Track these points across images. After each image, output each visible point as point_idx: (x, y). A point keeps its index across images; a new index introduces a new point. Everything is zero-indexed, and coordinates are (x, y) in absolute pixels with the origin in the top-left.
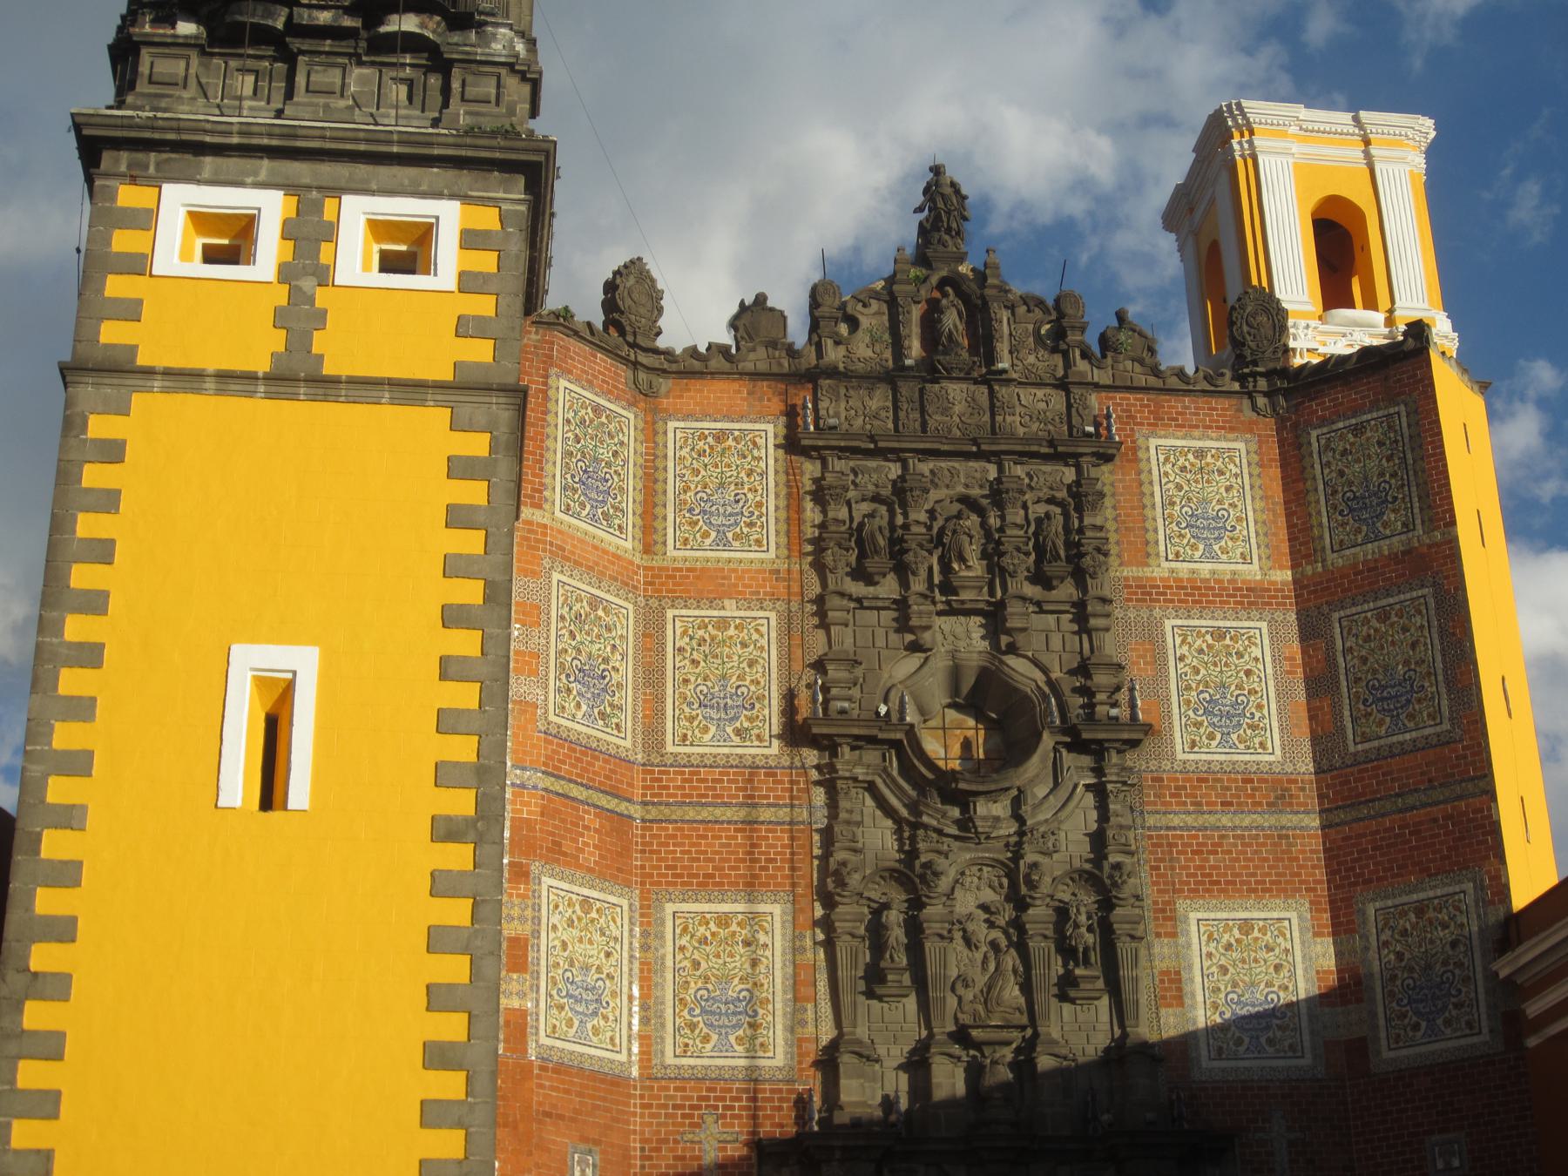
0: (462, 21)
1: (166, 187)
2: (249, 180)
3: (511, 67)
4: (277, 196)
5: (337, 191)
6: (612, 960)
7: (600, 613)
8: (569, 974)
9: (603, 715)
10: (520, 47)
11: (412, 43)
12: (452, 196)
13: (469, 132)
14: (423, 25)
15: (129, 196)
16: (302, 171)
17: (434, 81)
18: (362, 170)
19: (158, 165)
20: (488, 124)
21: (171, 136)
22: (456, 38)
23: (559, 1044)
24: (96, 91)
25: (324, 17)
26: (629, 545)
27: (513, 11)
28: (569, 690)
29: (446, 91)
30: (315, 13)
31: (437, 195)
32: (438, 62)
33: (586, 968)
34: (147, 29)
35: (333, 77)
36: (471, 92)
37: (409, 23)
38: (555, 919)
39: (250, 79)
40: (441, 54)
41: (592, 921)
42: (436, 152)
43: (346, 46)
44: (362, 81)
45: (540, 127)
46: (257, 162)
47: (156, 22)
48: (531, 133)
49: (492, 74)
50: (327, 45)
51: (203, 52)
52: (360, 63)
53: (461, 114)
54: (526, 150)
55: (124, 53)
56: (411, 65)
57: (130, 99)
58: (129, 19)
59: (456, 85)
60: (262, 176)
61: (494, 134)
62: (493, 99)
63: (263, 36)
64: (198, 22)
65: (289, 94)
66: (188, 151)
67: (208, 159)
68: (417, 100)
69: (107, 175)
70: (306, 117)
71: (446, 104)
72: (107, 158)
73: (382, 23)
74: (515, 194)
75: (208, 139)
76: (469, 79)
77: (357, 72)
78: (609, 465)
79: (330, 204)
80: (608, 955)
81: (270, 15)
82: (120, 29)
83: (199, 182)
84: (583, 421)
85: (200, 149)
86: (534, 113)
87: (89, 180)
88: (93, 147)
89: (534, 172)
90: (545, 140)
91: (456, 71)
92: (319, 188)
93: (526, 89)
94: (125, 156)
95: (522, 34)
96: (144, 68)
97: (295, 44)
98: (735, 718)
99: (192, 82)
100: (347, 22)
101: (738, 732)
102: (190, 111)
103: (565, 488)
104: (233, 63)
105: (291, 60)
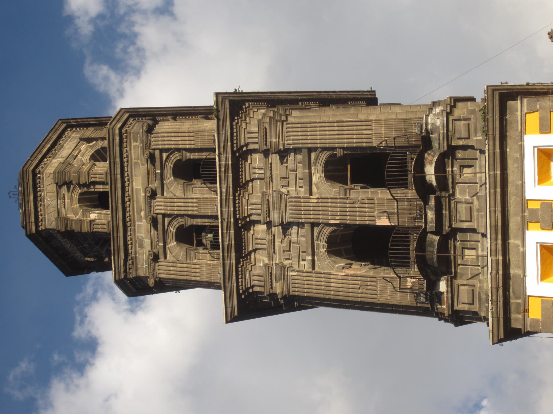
0: (426, 142)
1: (529, 293)
2: (521, 249)
3: (448, 114)
4: (528, 234)
5: (524, 202)
10: (437, 110)
11: (440, 168)
12: (522, 140)
13: (485, 133)
14: (431, 163)
15: (535, 312)
16: (514, 222)
17: (460, 154)
18: (511, 189)
19: (517, 298)
20: (481, 123)
21: (501, 292)
22: (435, 145)
24: (480, 332)
25: (431, 215)
27: (419, 115)
29: (465, 148)
30: (429, 220)
31: (522, 148)
32: (450, 153)
34: (445, 307)
35: (462, 208)
36: (464, 134)
37: (430, 170)
39: (467, 252)
40: (445, 151)
42: (498, 150)
43: (445, 203)
44: (463, 192)
45: (480, 95)
46: (511, 245)
47: (441, 302)
48: (483, 100)
49: (453, 124)
50: (445, 212)
51: (455, 277)
52: (454, 194)
53: (477, 139)
54: (493, 102)
55: (459, 318)
56: (452, 167)
57: (483, 314)
58: (440, 316)
59: (461, 143)
60: (519, 242)
61: (486, 120)
62: (467, 122)
63: (443, 246)
64: (439, 280)
65: (474, 231)
66: (507, 282)
67: (512, 272)
68: (470, 162)
69: (525, 325)
70: (485, 221)
71: (472, 147)
72: (515, 325)
73: (431, 185)
74: (517, 106)
75: (501, 272)
76: (457, 136)
77: (458, 196)
79: (531, 205)
81: (432, 243)
82: (446, 321)
83: (524, 276)
85: (506, 276)
86: (472, 99)
87: (528, 334)
88: (510, 332)
89: (505, 96)
90: (487, 92)
91: (454, 143)
92: (523, 211)
93: (459, 105)
94: (513, 316)
95: (431, 110)
96: (466, 307)
97: (446, 229)
99: (471, 282)
100: (432, 202)
102: (486, 282)
104: (459, 261)
105: (455, 231)
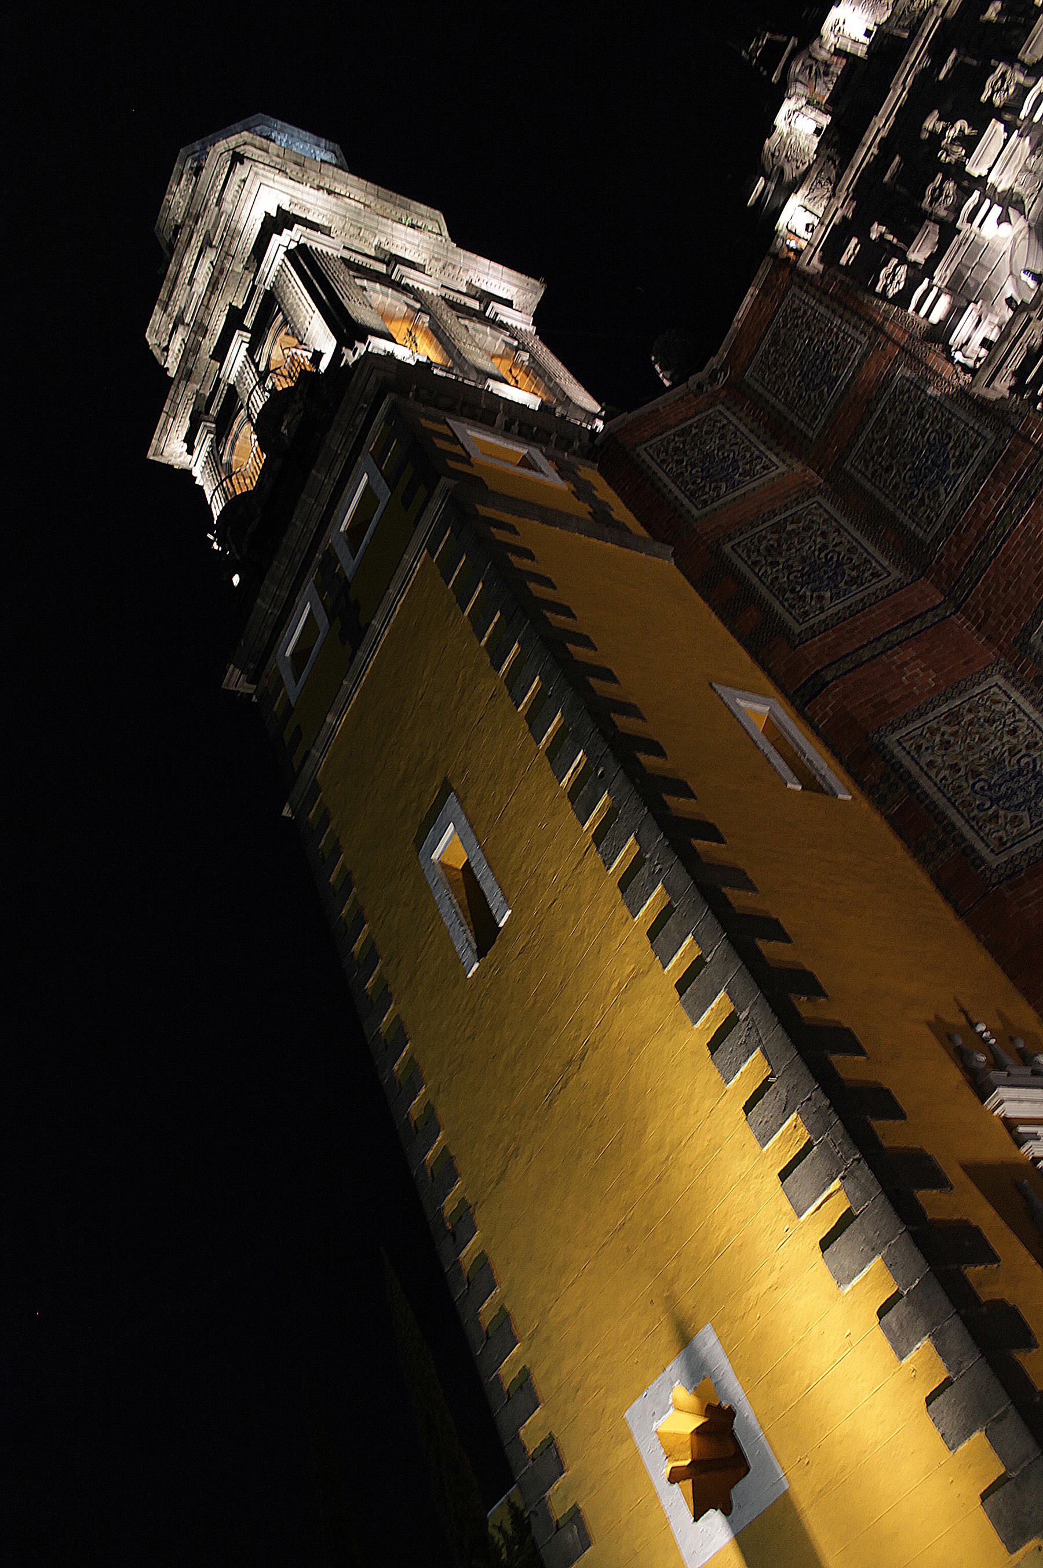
6: (1023, 730)
7: (789, 528)
8: (977, 787)
9: (852, 581)
23: (1017, 849)
26: (783, 468)
28: (803, 598)
33: (997, 763)
38: (927, 757)
41: (971, 723)
78: (721, 447)
80: (1013, 732)
84: (676, 449)
98: (946, 461)
101: (958, 464)
103: (691, 496)
